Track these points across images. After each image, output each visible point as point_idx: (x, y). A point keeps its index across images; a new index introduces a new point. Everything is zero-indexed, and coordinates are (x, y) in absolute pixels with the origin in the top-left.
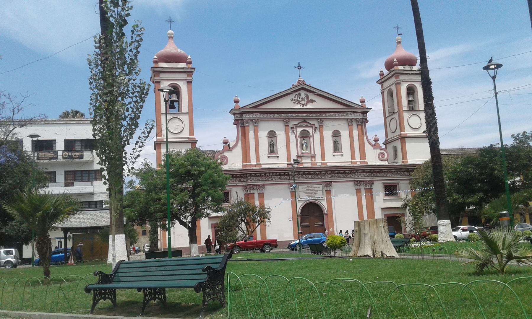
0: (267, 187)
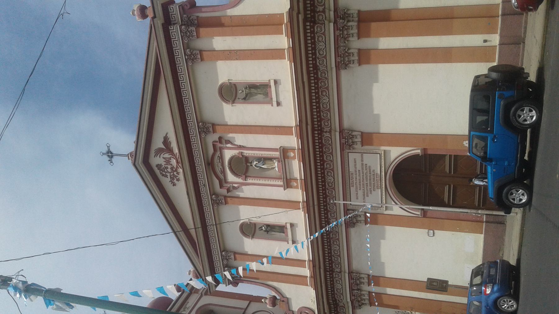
0: (355, 266)
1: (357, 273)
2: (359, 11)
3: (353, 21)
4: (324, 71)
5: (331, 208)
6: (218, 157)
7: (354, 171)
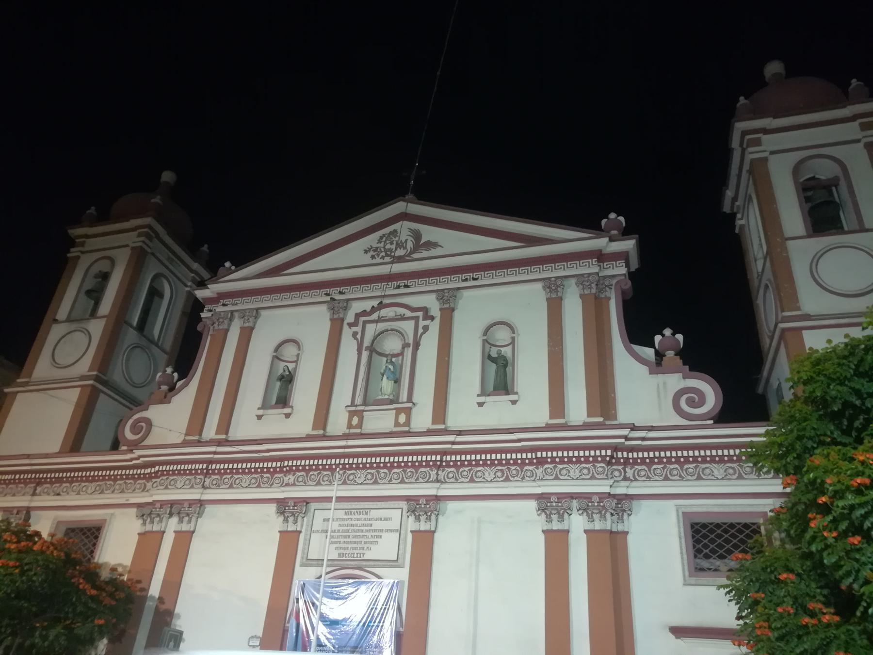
1: (198, 514)
2: (627, 533)
3: (613, 522)
4: (535, 475)
5: (313, 477)
6: (404, 315)
7: (370, 517)
